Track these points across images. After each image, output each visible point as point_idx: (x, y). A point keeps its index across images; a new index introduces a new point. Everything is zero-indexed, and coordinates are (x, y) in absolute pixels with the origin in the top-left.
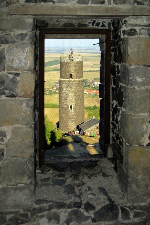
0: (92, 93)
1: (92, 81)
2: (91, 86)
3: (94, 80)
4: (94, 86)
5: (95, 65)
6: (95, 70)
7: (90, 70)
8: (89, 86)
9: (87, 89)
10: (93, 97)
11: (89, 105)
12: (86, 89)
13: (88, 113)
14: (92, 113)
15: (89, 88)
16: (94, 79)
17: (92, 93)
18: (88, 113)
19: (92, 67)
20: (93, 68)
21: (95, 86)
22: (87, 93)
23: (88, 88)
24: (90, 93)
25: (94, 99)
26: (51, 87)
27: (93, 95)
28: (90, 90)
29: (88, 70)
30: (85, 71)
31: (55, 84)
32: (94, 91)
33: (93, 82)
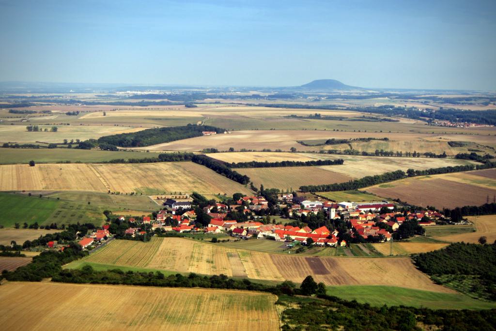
0: (293, 237)
1: (294, 195)
2: (291, 214)
3: (299, 195)
4: (300, 214)
5: (302, 143)
6: (304, 160)
7: (286, 160)
8: (284, 213)
9: (277, 221)
10: (297, 252)
11: (283, 280)
12: (274, 222)
13: (281, 308)
14: (295, 306)
15: (288, 221)
16: (303, 189)
17: (293, 237)
18: (281, 308)
19: (293, 150)
20: (293, 154)
21: (305, 213)
22: (277, 237)
23: (278, 219)
24: (285, 236)
25: (302, 257)
26: (146, 214)
27: (297, 245)
28: (286, 225)
29: (280, 160)
30: (269, 162)
31: (165, 204)
32: (302, 231)
33: (297, 200)
